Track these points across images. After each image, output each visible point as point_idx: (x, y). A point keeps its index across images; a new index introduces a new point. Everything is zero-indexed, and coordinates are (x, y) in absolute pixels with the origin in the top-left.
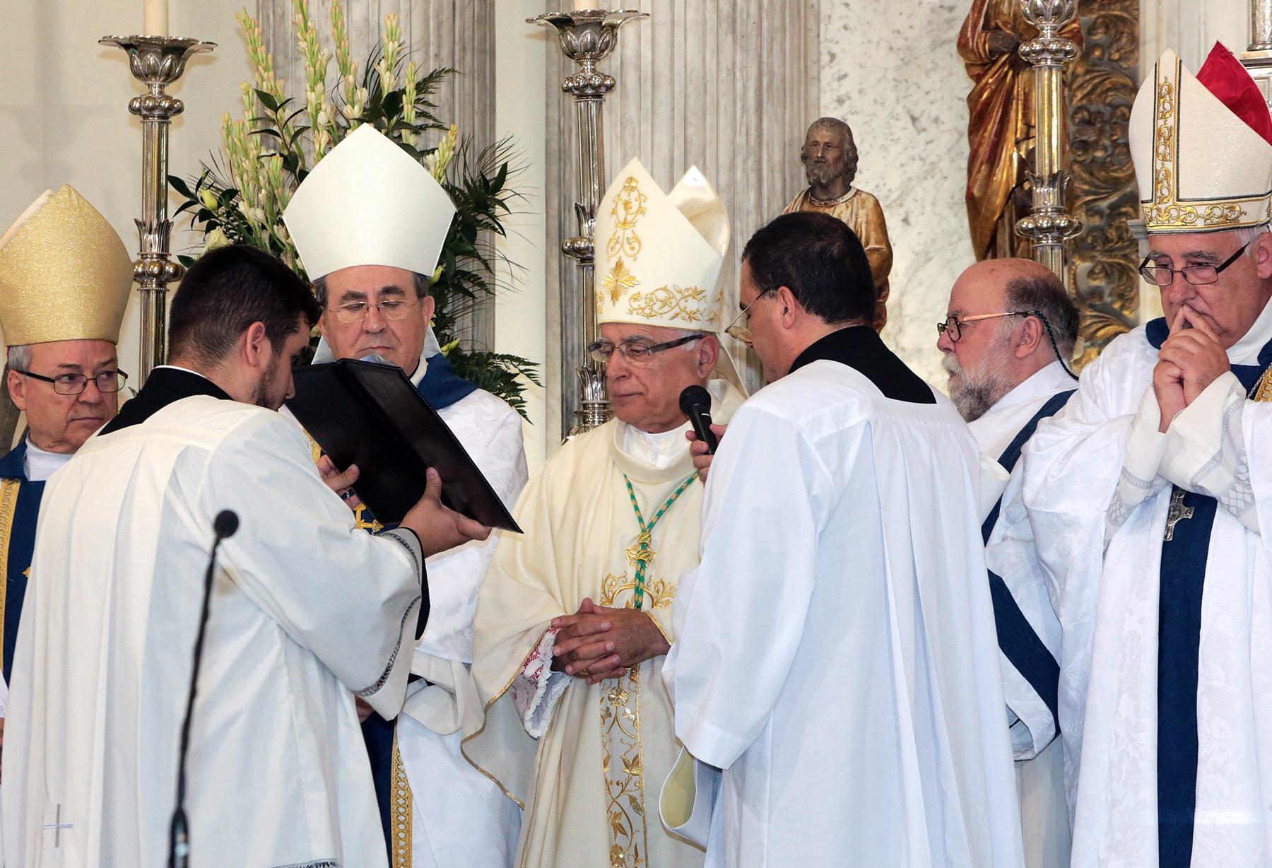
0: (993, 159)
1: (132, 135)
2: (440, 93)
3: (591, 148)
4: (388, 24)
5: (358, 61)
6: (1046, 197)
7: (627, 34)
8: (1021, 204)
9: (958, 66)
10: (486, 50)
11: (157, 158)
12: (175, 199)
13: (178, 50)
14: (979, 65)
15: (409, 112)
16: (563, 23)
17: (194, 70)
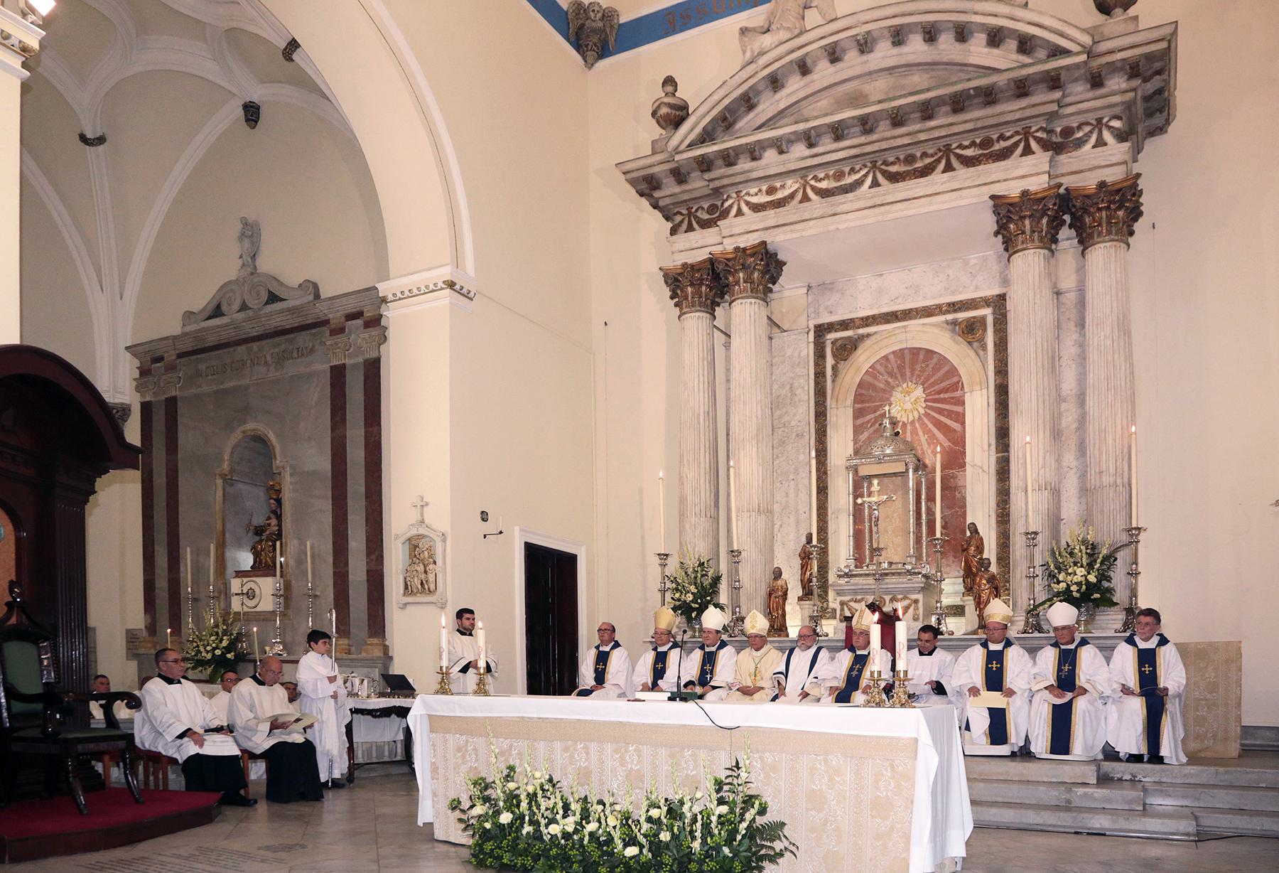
0: (805, 574)
1: (659, 569)
2: (711, 562)
3: (737, 571)
4: (702, 550)
5: (697, 557)
6: (814, 580)
7: (743, 553)
8: (810, 581)
9: (799, 558)
10: (718, 555)
11: (663, 572)
12: (666, 578)
13: (667, 555)
14: (802, 559)
15: (706, 565)
16: (732, 551)
17: (669, 558)
